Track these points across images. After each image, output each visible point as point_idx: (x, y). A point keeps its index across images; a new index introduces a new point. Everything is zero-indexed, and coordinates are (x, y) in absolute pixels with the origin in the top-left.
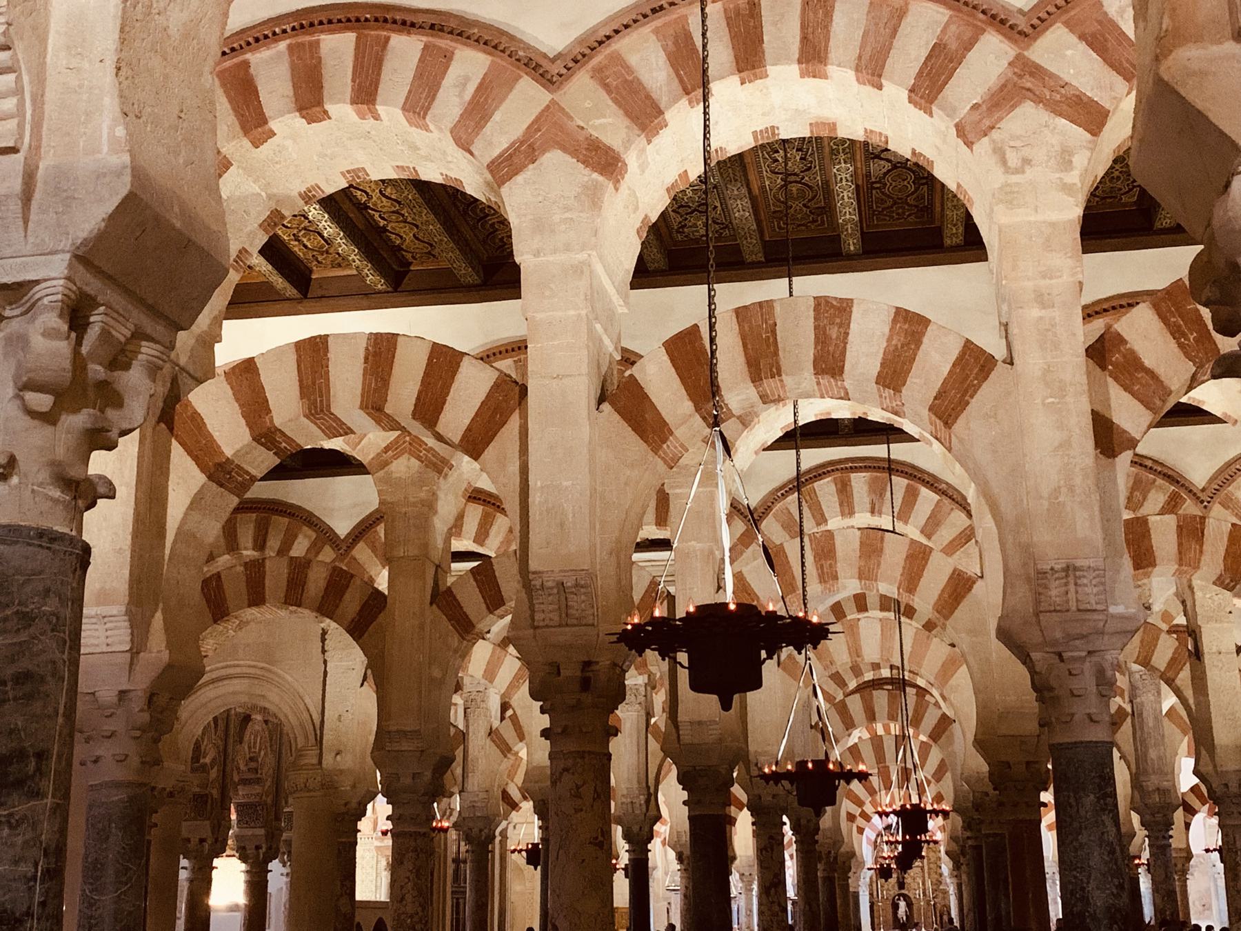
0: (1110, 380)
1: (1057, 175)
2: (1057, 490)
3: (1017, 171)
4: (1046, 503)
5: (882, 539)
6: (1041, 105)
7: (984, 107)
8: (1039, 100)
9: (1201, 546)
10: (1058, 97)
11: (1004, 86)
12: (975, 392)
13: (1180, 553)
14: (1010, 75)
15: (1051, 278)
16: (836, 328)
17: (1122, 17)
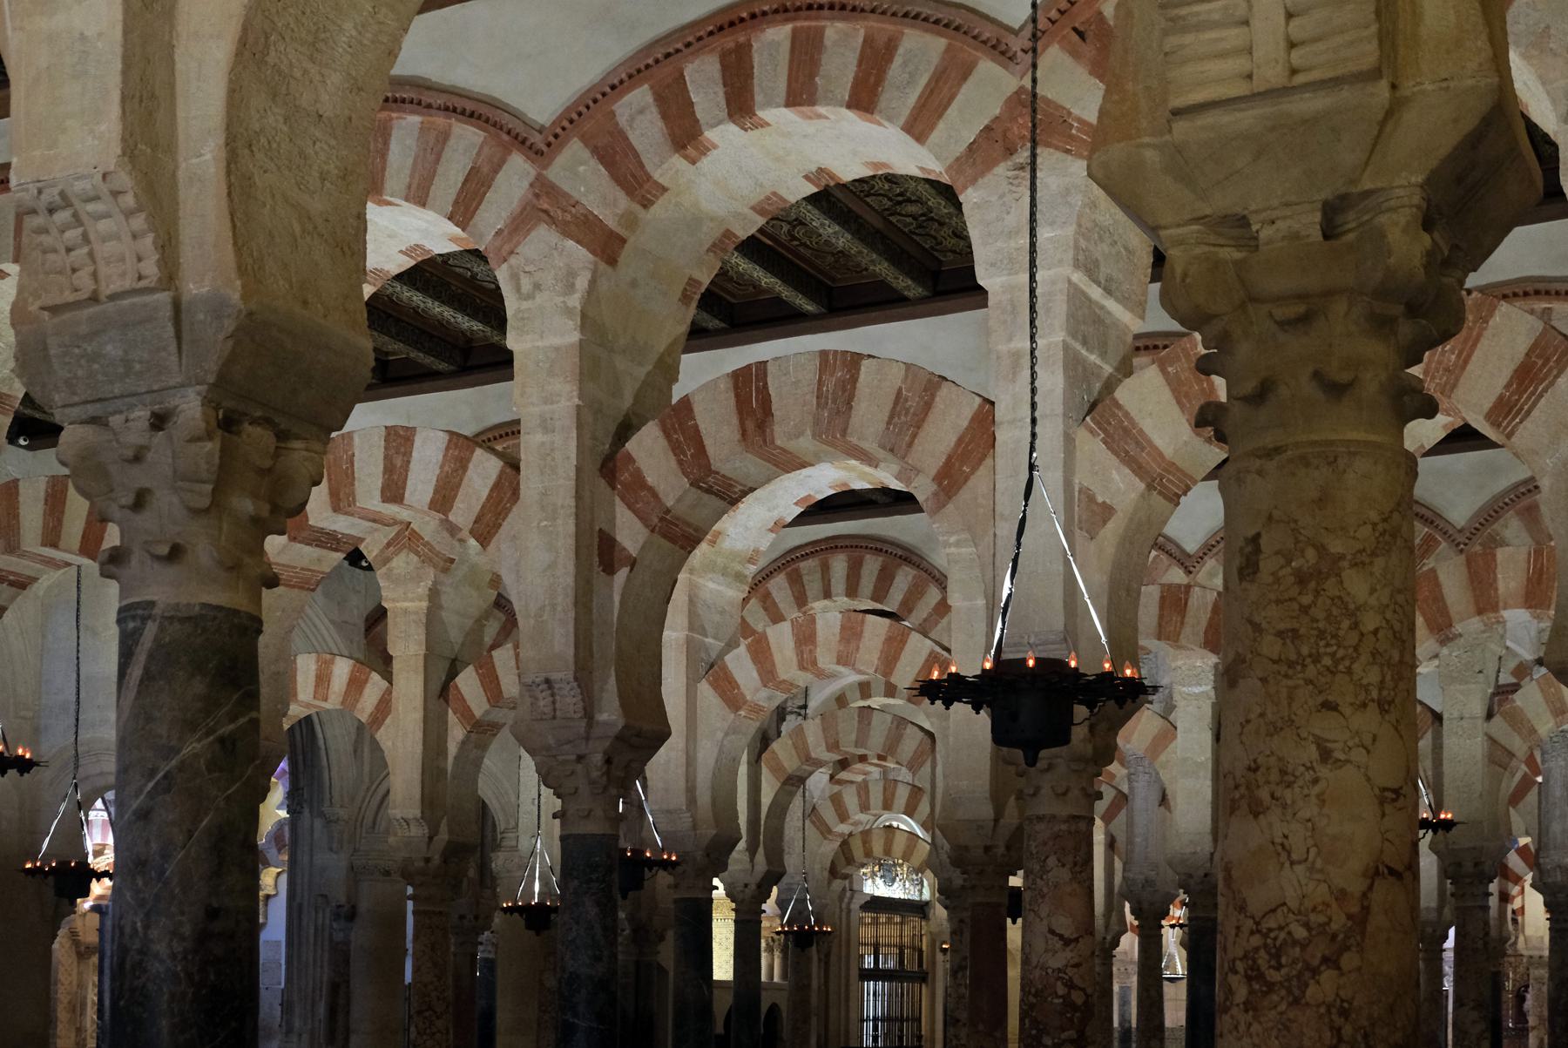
0: (617, 499)
1: (562, 299)
2: (542, 608)
3: (530, 297)
4: (532, 621)
5: (863, 621)
6: (554, 227)
7: (506, 232)
8: (552, 221)
9: (1183, 617)
10: (568, 217)
11: (524, 209)
12: (507, 515)
13: (1160, 625)
14: (530, 196)
15: (552, 403)
16: (401, 458)
17: (631, 126)
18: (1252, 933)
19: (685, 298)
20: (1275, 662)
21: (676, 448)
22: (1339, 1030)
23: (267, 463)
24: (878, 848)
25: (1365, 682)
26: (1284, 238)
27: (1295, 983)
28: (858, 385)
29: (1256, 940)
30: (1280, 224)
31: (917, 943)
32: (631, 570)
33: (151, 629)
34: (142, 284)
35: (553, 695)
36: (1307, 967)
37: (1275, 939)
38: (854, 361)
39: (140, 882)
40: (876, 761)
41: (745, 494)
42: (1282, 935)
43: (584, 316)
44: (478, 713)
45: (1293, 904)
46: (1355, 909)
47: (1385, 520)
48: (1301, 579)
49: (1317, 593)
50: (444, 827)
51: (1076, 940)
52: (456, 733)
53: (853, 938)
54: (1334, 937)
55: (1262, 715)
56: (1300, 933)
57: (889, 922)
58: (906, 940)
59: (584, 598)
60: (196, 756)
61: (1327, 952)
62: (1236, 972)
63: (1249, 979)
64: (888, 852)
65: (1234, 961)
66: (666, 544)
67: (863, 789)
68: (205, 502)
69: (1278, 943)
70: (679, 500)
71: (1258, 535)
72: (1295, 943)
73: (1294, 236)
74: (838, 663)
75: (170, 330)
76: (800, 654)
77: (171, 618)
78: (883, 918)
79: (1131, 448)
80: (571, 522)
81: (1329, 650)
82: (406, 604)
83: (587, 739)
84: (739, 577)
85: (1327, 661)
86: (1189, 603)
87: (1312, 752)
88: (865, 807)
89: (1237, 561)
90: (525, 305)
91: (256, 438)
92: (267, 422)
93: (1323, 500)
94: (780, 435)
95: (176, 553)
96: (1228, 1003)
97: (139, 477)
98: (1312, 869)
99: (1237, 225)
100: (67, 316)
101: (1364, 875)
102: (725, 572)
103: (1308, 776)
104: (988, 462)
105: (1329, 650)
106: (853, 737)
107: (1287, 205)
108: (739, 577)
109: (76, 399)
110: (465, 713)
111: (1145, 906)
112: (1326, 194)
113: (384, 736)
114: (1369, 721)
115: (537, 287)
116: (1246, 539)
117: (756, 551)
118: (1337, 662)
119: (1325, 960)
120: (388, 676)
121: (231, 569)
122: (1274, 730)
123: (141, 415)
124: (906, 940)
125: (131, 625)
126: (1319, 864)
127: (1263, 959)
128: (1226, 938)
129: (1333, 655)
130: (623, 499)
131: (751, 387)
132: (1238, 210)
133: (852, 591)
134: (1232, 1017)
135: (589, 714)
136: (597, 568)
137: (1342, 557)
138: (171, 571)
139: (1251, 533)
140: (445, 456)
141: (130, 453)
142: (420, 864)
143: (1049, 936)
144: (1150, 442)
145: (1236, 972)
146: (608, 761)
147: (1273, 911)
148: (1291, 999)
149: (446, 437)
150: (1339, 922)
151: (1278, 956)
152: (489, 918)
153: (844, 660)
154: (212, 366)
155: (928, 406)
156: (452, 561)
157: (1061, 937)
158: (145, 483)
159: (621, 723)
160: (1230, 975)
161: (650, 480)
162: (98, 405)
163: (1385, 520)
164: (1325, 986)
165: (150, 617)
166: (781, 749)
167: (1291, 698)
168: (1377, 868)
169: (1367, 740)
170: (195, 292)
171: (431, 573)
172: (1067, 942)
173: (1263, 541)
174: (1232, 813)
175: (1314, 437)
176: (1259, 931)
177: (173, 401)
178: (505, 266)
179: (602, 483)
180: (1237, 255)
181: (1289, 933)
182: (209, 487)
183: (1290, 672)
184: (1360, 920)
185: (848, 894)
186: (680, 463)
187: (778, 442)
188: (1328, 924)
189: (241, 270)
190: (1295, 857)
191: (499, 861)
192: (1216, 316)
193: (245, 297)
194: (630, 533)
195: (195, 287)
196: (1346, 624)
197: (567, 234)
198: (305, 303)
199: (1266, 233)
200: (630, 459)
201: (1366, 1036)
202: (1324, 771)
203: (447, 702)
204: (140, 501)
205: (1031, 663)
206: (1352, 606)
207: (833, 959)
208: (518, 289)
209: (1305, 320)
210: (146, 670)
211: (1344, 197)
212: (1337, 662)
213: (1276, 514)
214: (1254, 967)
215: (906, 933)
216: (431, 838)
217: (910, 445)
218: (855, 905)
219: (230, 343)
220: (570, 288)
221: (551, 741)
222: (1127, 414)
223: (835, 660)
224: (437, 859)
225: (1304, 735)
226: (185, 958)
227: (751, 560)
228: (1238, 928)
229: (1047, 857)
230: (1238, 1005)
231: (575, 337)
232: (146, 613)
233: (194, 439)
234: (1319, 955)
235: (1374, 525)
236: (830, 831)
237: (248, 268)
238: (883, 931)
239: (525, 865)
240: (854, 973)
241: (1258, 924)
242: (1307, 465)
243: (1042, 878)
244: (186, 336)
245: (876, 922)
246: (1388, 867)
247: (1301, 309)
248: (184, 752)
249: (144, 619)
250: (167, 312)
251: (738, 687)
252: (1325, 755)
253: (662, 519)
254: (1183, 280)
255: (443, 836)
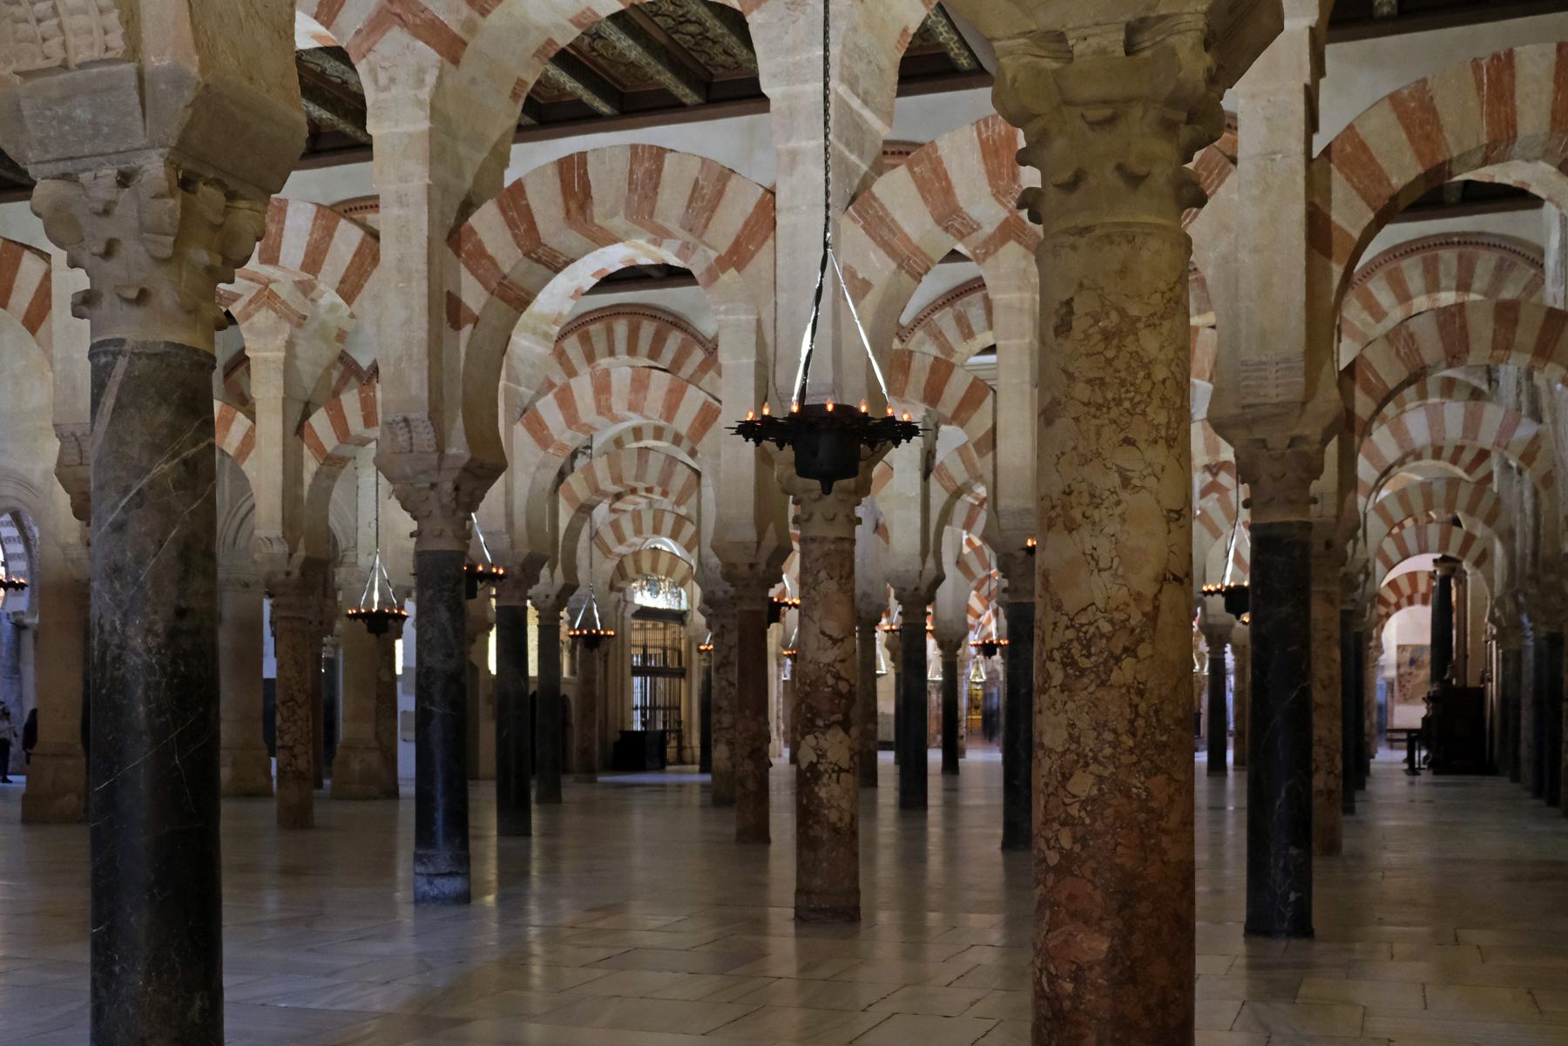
0: (462, 266)
1: (413, 92)
2: (400, 359)
3: (386, 89)
4: (392, 368)
8: (405, 24)
10: (418, 21)
11: (379, 13)
15: (406, 182)
18: (1067, 628)
19: (515, 95)
20: (1085, 404)
21: (512, 224)
22: (1137, 706)
23: (219, 220)
24: (646, 565)
25: (1155, 422)
26: (1094, 52)
27: (1102, 668)
28: (663, 174)
29: (1070, 634)
30: (1090, 40)
31: (677, 644)
32: (475, 327)
33: (121, 364)
34: (110, 55)
35: (410, 432)
36: (1112, 655)
37: (1086, 633)
38: (659, 154)
39: (117, 585)
40: (644, 494)
41: (567, 264)
42: (1092, 630)
43: (432, 107)
44: (329, 447)
45: (1100, 604)
46: (1148, 608)
47: (1171, 290)
48: (1107, 336)
49: (1119, 348)
50: (301, 545)
51: (842, 640)
52: (311, 465)
53: (626, 639)
54: (1133, 630)
55: (1075, 448)
56: (1106, 628)
57: (655, 627)
58: (668, 643)
59: (435, 349)
60: (164, 475)
61: (1127, 644)
62: (1053, 660)
63: (1065, 665)
64: (654, 569)
65: (1052, 651)
66: (504, 306)
67: (637, 516)
68: (167, 252)
69: (1088, 636)
70: (514, 268)
71: (1072, 299)
72: (1102, 636)
73: (1102, 51)
74: (629, 409)
75: (135, 98)
76: (598, 401)
77: (139, 355)
78: (649, 624)
79: (887, 236)
80: (424, 284)
81: (1129, 395)
82: (266, 354)
83: (439, 469)
84: (546, 336)
85: (1127, 405)
86: (912, 365)
87: (1115, 479)
88: (638, 531)
89: (1054, 320)
90: (383, 96)
91: (209, 196)
92: (218, 183)
93: (1123, 272)
94: (598, 213)
95: (143, 297)
96: (1046, 685)
97: (109, 229)
98: (1115, 575)
99: (1057, 39)
100: (38, 81)
101: (1156, 580)
102: (534, 332)
103: (1114, 498)
104: (770, 242)
105: (1129, 395)
106: (634, 472)
107: (1097, 24)
108: (546, 336)
109: (49, 157)
110: (318, 448)
111: (863, 614)
112: (1129, 17)
113: (248, 467)
114: (1158, 455)
115: (392, 80)
116: (1061, 303)
117: (560, 314)
118: (1135, 405)
119: (1126, 650)
120: (251, 415)
121: (189, 312)
122: (1086, 461)
123: (109, 173)
124: (668, 643)
125: (103, 360)
126: (1120, 572)
127: (1076, 649)
128: (1044, 632)
129: (1132, 400)
130: (467, 266)
131: (572, 173)
132: (1058, 27)
133: (632, 350)
134: (1050, 697)
135: (440, 449)
136: (446, 325)
137: (1139, 319)
138: (138, 313)
139: (1065, 298)
140: (314, 225)
141: (100, 207)
142: (282, 577)
143: (821, 637)
144: (901, 231)
145: (1053, 660)
146: (457, 489)
147: (1085, 609)
148: (1099, 681)
149: (314, 208)
150: (1136, 619)
151: (1088, 647)
152: (331, 625)
153: (633, 407)
154: (173, 132)
155: (720, 194)
156: (305, 318)
157: (830, 637)
158: (115, 235)
159: (467, 456)
160: (1048, 662)
161: (490, 250)
162: (69, 163)
163: (1171, 290)
164: (1126, 671)
165: (120, 353)
166: (575, 481)
167: (1099, 434)
168: (1165, 575)
169: (1158, 469)
170: (156, 64)
171: (286, 328)
172: (835, 641)
173: (1076, 305)
174: (1048, 529)
175: (1116, 220)
176: (1073, 626)
177: (137, 162)
178: (364, 61)
179: (450, 252)
180: (1055, 65)
181: (1097, 628)
182: (172, 239)
183: (1098, 413)
184: (1152, 617)
185: (622, 604)
186: (515, 236)
187: (597, 221)
188: (1128, 620)
189: (198, 46)
190: (1102, 565)
191: (341, 575)
192: (1039, 115)
193: (203, 70)
194: (473, 295)
195: (156, 60)
196: (1141, 374)
197: (417, 36)
198: (251, 79)
199: (1079, 48)
200: (472, 231)
201: (1157, 712)
202: (1125, 495)
203: (302, 437)
204: (110, 250)
205: (830, 408)
206: (1146, 360)
207: (611, 658)
208: (376, 81)
209: (1111, 121)
210: (118, 399)
211: (1143, 20)
212: (1135, 405)
213: (1086, 282)
214: (1069, 655)
215: (668, 637)
216: (290, 555)
217: (706, 226)
218: (628, 614)
219: (190, 111)
220: (421, 82)
221: (408, 471)
222: (882, 206)
223: (627, 407)
224: (296, 573)
225: (1109, 465)
226: (159, 652)
227: (555, 322)
228: (1055, 624)
229: (818, 572)
230: (1055, 687)
231: (425, 125)
232: (117, 349)
233: (159, 196)
234: (1121, 646)
235: (1163, 293)
236: (610, 552)
237: (204, 44)
238: (650, 635)
239: (365, 580)
240: (628, 671)
241: (1072, 620)
242: (1112, 243)
243: (814, 589)
244: (149, 103)
245: (643, 628)
246: (1172, 574)
247: (1106, 112)
248: (154, 471)
249: (115, 355)
250: (133, 82)
251: (547, 428)
252: (1126, 482)
253: (500, 284)
254: (1013, 84)
255: (301, 554)
